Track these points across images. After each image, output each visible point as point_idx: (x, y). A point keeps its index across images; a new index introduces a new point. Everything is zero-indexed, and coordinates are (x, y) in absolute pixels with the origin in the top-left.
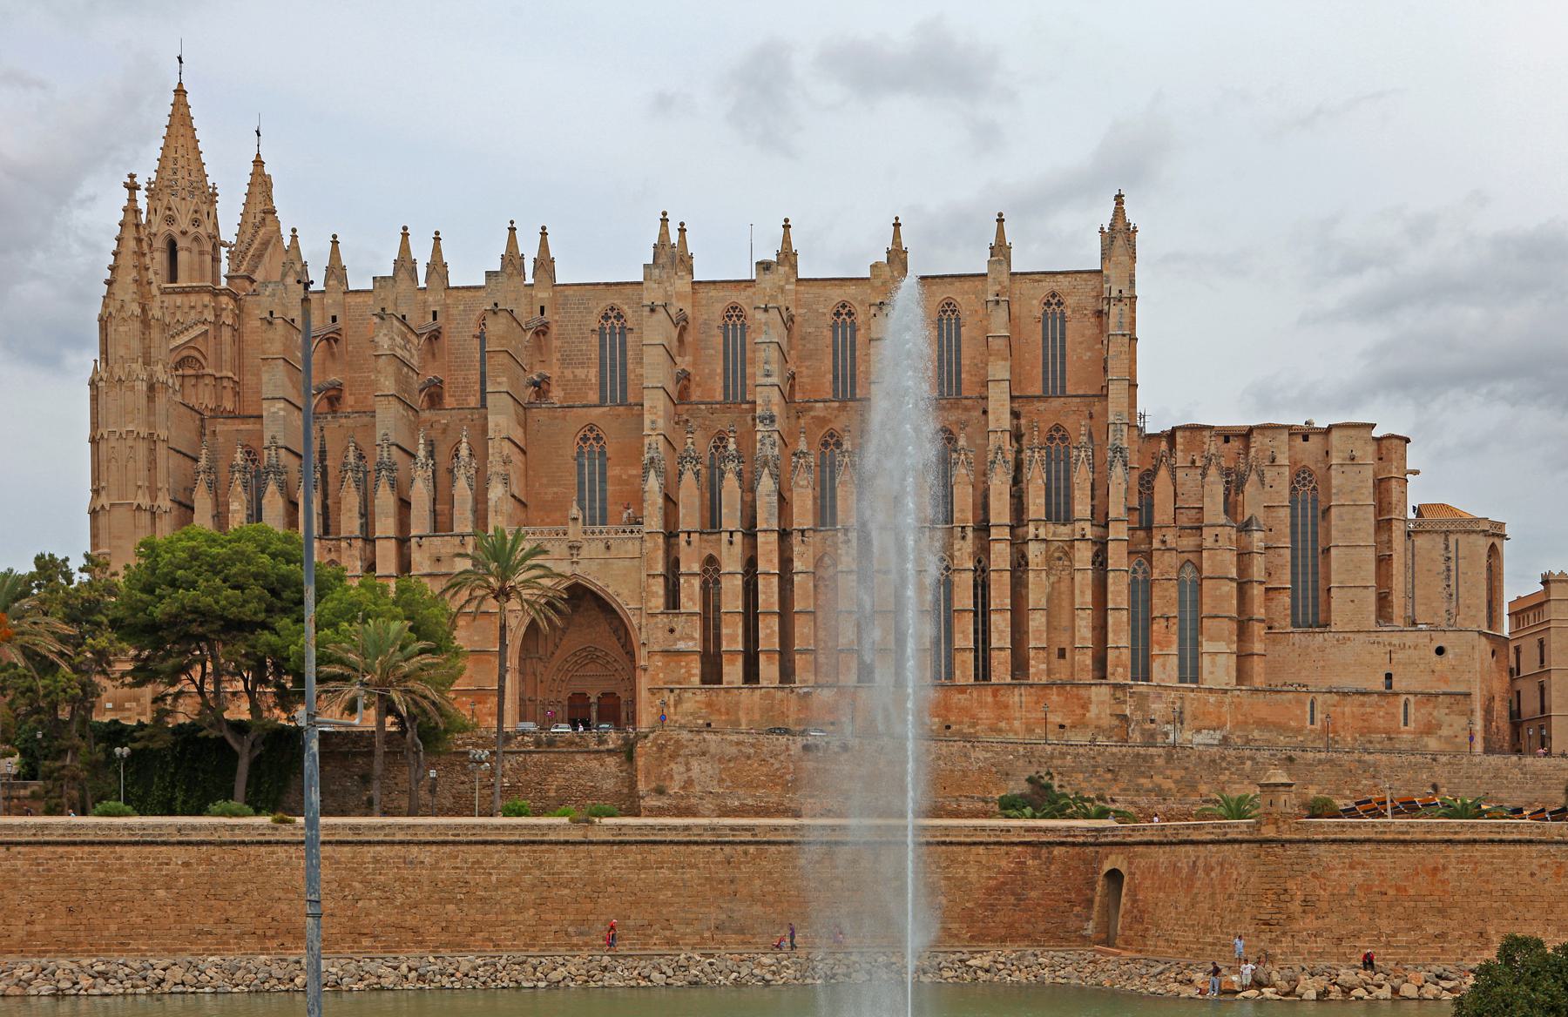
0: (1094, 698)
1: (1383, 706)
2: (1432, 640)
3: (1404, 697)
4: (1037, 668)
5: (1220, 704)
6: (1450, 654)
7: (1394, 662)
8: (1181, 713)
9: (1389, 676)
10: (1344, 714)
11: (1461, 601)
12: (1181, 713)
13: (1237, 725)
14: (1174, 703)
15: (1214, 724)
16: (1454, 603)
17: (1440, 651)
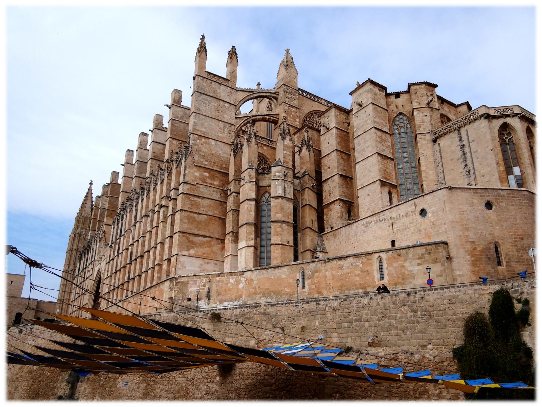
0: (165, 290)
1: (358, 266)
2: (416, 206)
3: (377, 255)
4: (156, 275)
5: (238, 282)
6: (429, 214)
7: (395, 230)
8: (209, 292)
9: (393, 243)
10: (325, 277)
11: (477, 173)
12: (209, 292)
13: (250, 295)
14: (204, 286)
15: (233, 297)
16: (473, 177)
17: (423, 212)
